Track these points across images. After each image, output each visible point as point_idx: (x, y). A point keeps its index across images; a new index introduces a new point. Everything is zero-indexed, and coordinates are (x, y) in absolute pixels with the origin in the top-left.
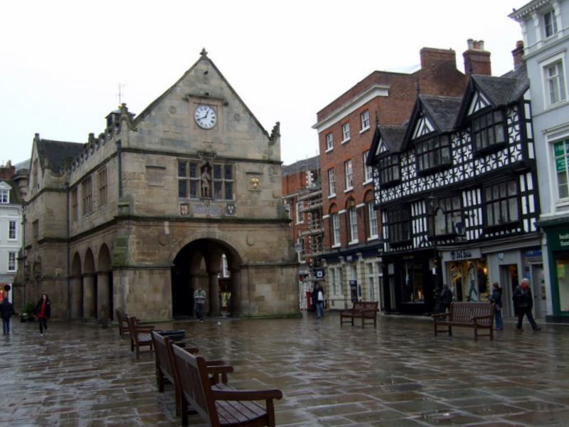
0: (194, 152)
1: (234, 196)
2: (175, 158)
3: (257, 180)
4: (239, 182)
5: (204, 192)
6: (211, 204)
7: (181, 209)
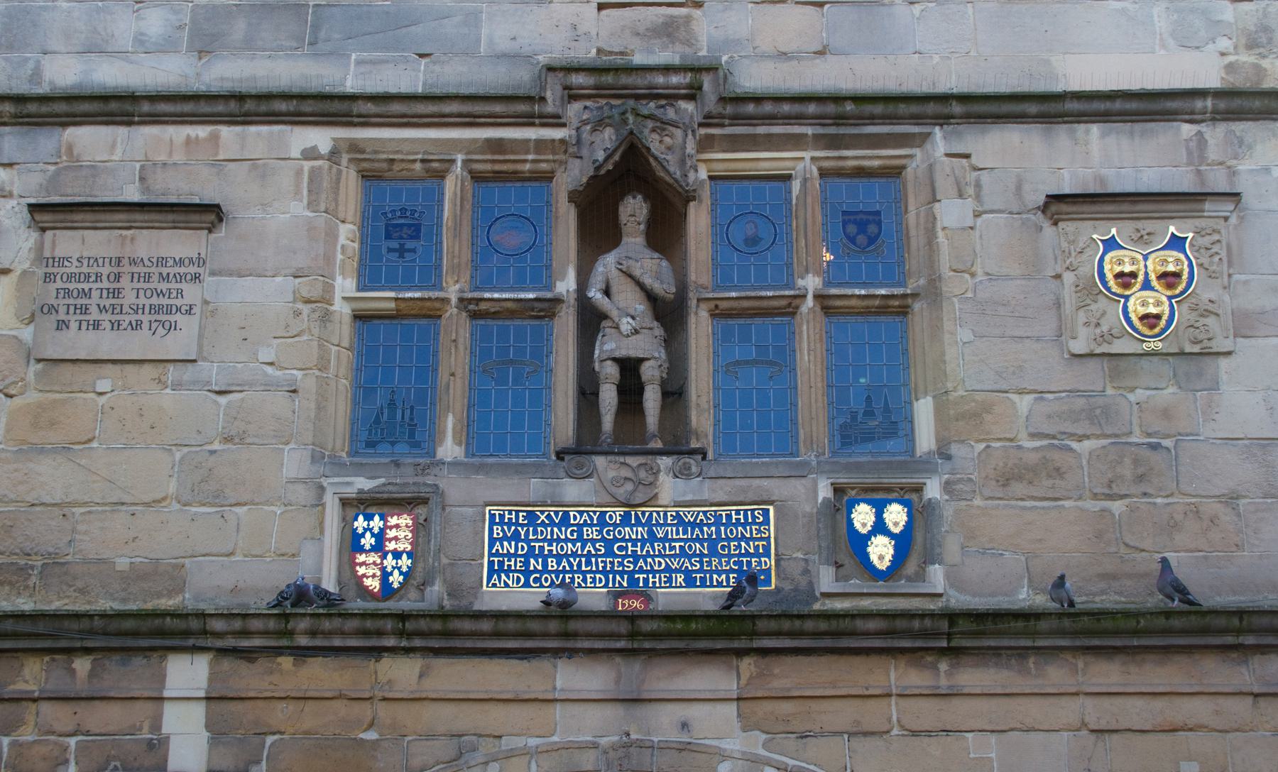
0: (520, 78)
1: (924, 411)
2: (322, 138)
3: (1172, 261)
4: (953, 286)
5: (608, 396)
6: (669, 487)
7: (353, 544)
